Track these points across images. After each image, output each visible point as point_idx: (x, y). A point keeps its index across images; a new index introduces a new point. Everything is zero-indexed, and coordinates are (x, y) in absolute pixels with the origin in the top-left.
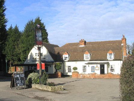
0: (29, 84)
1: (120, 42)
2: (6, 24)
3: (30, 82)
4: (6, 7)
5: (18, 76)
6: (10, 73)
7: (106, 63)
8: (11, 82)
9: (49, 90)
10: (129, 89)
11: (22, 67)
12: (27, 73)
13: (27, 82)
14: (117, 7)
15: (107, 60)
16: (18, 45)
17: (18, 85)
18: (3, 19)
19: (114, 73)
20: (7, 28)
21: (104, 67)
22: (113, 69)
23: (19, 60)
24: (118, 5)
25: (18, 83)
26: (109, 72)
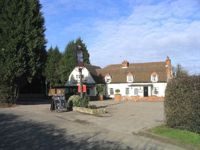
0: (70, 107)
1: (164, 63)
2: (46, 45)
3: (71, 104)
4: (46, 28)
5: (58, 98)
6: (50, 95)
7: (149, 85)
8: (51, 105)
9: (91, 113)
10: (173, 112)
11: (62, 89)
12: (67, 96)
13: (67, 104)
14: (161, 28)
15: (151, 82)
16: (58, 66)
17: (59, 108)
18: (43, 39)
19: (158, 95)
20: (47, 49)
21: (147, 90)
22: (157, 92)
23: (60, 82)
24: (162, 25)
25: (59, 106)
26: (153, 94)
